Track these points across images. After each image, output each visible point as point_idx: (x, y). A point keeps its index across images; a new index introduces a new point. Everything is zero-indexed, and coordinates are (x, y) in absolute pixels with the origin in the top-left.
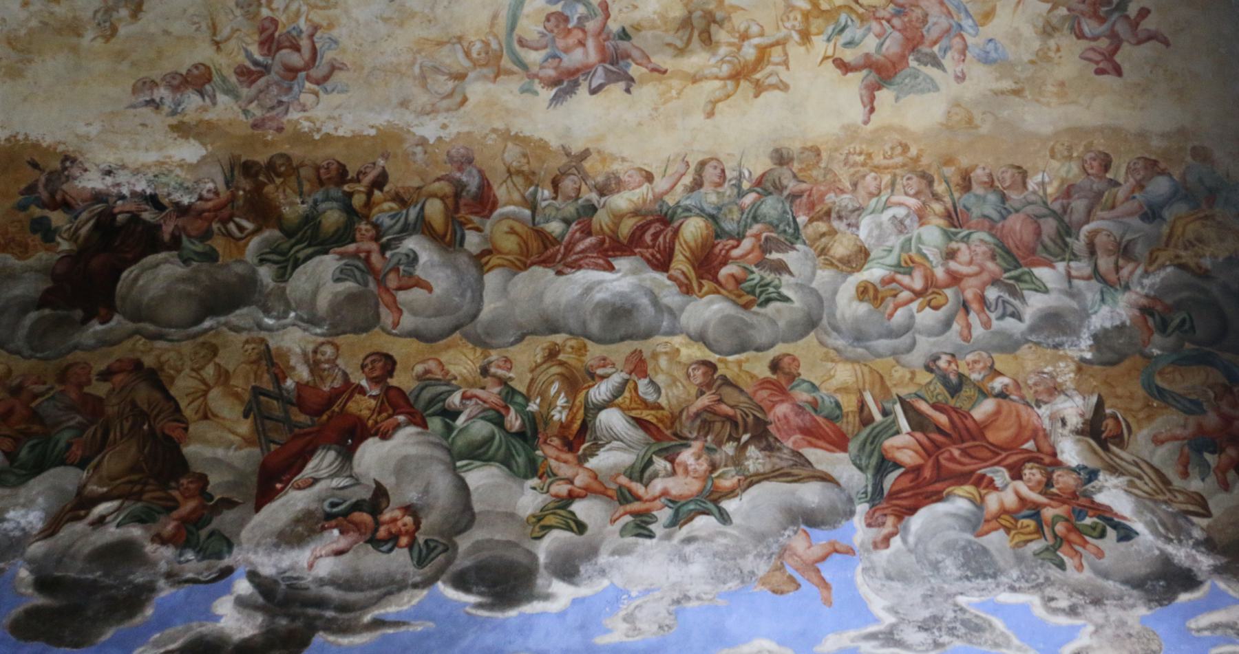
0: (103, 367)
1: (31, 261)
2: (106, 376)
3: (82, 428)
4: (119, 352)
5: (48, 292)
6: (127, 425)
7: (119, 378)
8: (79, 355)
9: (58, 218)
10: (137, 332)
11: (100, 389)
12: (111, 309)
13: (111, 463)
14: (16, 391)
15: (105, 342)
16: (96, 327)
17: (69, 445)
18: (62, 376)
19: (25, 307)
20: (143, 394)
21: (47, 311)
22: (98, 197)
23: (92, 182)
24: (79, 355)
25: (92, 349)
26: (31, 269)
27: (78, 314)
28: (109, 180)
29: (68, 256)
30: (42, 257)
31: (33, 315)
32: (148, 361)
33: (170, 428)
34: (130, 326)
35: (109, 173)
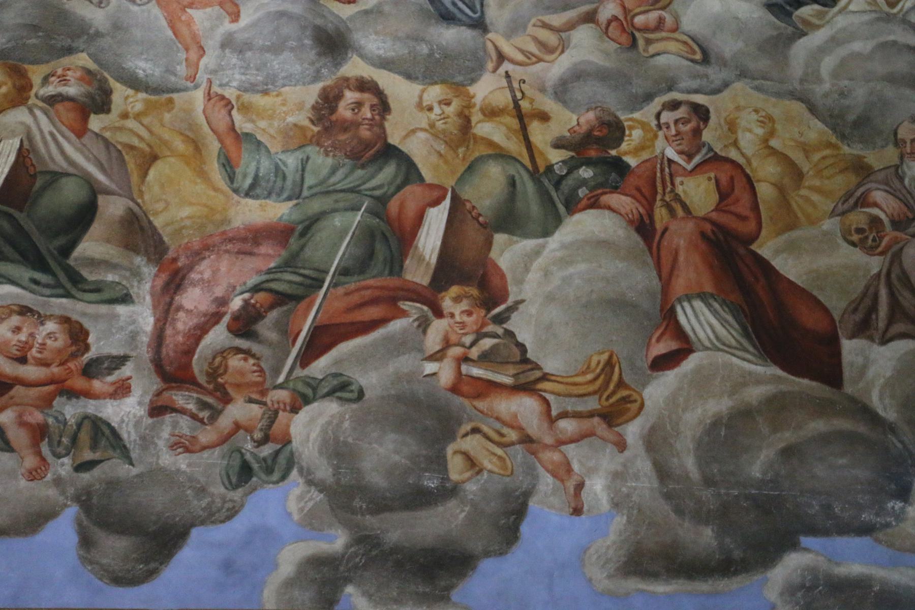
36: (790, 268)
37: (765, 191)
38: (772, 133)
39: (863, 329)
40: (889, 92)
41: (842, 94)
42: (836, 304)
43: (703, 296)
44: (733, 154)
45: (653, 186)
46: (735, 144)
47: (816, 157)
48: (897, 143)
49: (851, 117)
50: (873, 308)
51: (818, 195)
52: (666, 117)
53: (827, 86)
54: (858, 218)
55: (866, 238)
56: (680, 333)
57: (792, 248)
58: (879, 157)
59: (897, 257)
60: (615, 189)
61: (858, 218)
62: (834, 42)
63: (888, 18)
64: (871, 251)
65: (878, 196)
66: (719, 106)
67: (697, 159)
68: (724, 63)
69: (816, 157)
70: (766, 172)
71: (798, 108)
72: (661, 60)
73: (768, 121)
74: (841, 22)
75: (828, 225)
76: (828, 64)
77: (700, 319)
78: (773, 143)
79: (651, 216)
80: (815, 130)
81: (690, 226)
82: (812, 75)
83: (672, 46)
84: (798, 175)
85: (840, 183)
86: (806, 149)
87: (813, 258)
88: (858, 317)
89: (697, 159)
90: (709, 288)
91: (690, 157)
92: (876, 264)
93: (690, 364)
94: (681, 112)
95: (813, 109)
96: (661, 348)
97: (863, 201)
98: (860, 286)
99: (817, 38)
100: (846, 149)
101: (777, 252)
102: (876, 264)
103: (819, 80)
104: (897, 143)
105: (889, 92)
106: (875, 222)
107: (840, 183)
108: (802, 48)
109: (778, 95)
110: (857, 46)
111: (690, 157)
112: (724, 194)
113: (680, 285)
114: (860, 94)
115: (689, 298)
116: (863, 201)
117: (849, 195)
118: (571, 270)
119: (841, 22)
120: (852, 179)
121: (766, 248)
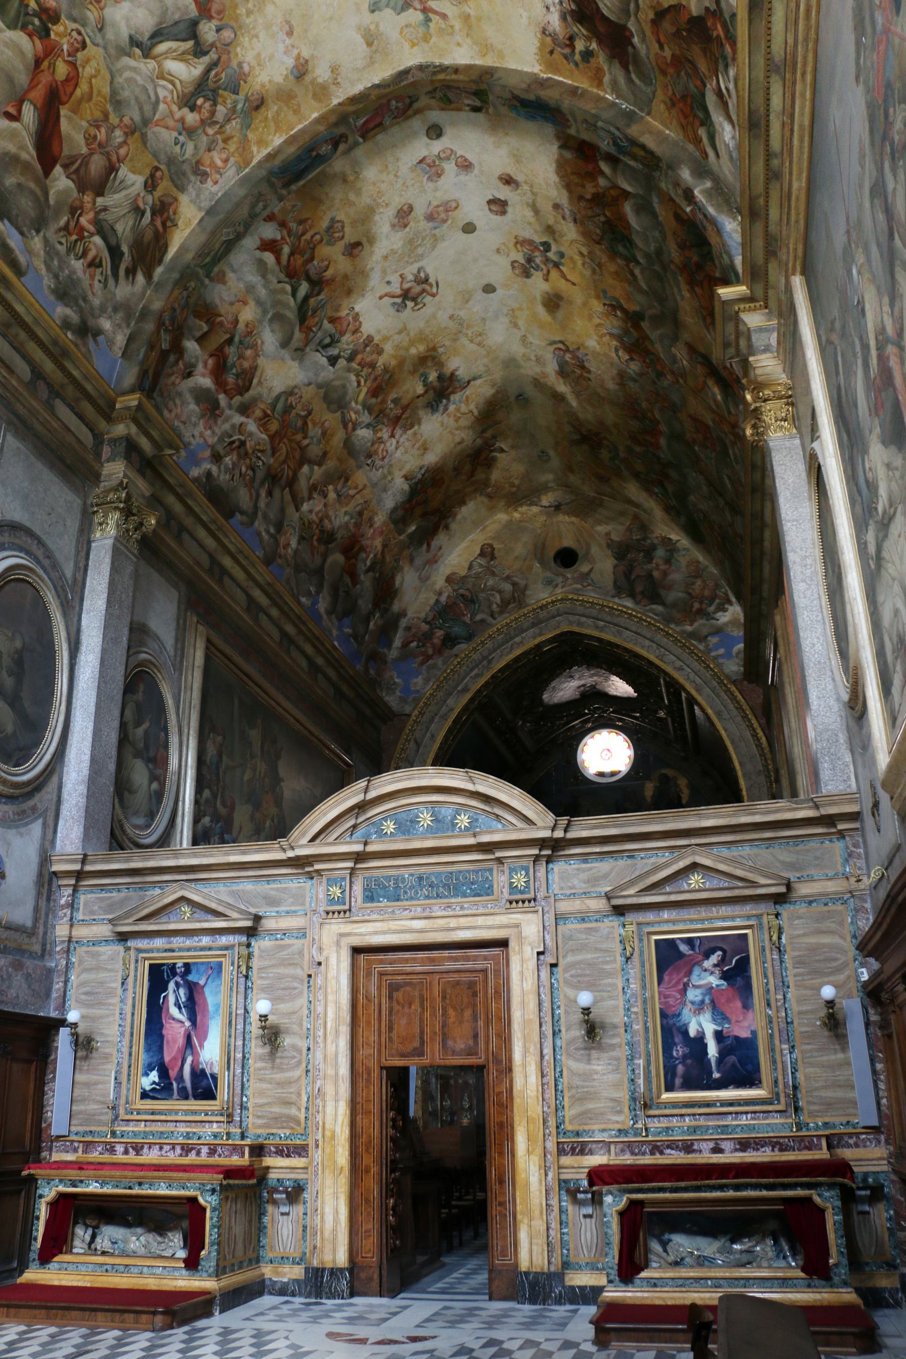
0: (657, 46)
1: (606, 68)
2: (661, 47)
3: (688, 75)
4: (648, 33)
5: (620, 63)
6: (684, 45)
7: (662, 39)
8: (652, 57)
9: (580, 45)
10: (636, 15)
11: (667, 53)
12: (624, 28)
13: (703, 67)
14: (673, 105)
15: (643, 40)
16: (636, 40)
17: (695, 86)
18: (664, 73)
19: (630, 81)
20: (667, 26)
21: (631, 68)
22: (563, 18)
23: (555, 20)
24: (652, 57)
25: (648, 48)
26: (609, 69)
27: (630, 49)
28: (552, 9)
29: (600, 42)
30: (601, 59)
31: (633, 76)
32: (651, 15)
33: (684, 18)
34: (632, 18)
35: (548, 8)
36: (64, 125)
37: (78, 92)
38: (95, 76)
39: (65, 167)
40: (133, 102)
41: (122, 88)
42: (66, 152)
43: (35, 107)
44: (80, 70)
45: (50, 51)
46: (84, 67)
47: (99, 99)
48: (121, 121)
49: (118, 98)
50: (73, 163)
51: (90, 111)
52: (74, 34)
53: (121, 80)
54: (93, 131)
55: (90, 139)
56: (19, 111)
57: (69, 119)
58: (114, 119)
59: (91, 154)
60: (40, 38)
61: (93, 131)
62: (135, 69)
63: (153, 81)
64: (87, 145)
65: (103, 130)
66: (91, 49)
67: (70, 59)
68: (103, 38)
69: (99, 99)
70: (83, 87)
71: (108, 77)
72: (89, 13)
73: (98, 71)
74: (142, 66)
75: (84, 124)
76: (127, 74)
77: (29, 113)
78: (93, 80)
79: (43, 61)
80: (106, 90)
81: (50, 79)
82: (121, 72)
83: (96, 13)
84: (90, 99)
85: (98, 114)
86: (99, 92)
87: (72, 129)
88: (67, 161)
89: (70, 59)
90: (39, 105)
91: (69, 55)
92: (84, 150)
93: (15, 125)
94: (79, 38)
95: (112, 83)
96: (12, 110)
97: (98, 127)
98: (75, 152)
99: (132, 62)
100: (108, 106)
101: (65, 116)
102: (84, 150)
103: (121, 76)
104: (121, 121)
105: (133, 102)
106: (95, 137)
107: (98, 114)
108: (126, 61)
109: (108, 67)
110: (138, 78)
111: (69, 55)
112: (67, 80)
113: (33, 95)
114: (126, 94)
115: (32, 103)
116: (98, 127)
117: (96, 121)
118: (6, 50)
119: (142, 66)
120: (102, 117)
121: (64, 111)
